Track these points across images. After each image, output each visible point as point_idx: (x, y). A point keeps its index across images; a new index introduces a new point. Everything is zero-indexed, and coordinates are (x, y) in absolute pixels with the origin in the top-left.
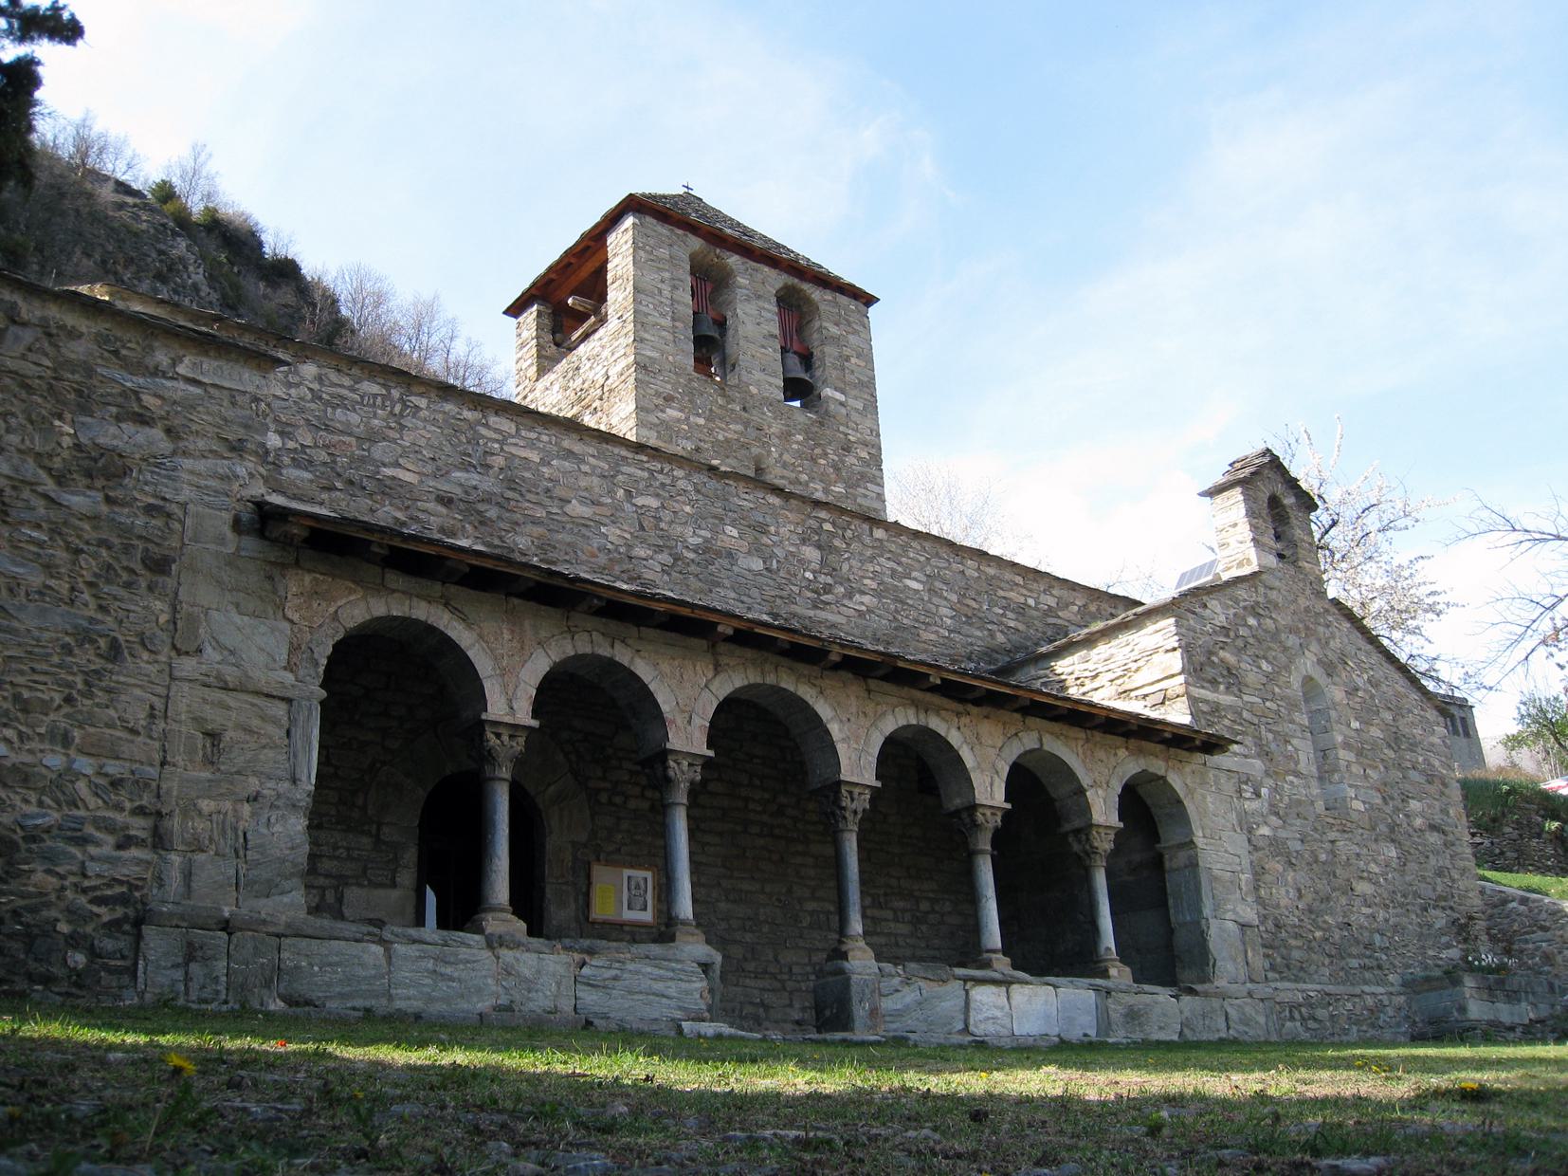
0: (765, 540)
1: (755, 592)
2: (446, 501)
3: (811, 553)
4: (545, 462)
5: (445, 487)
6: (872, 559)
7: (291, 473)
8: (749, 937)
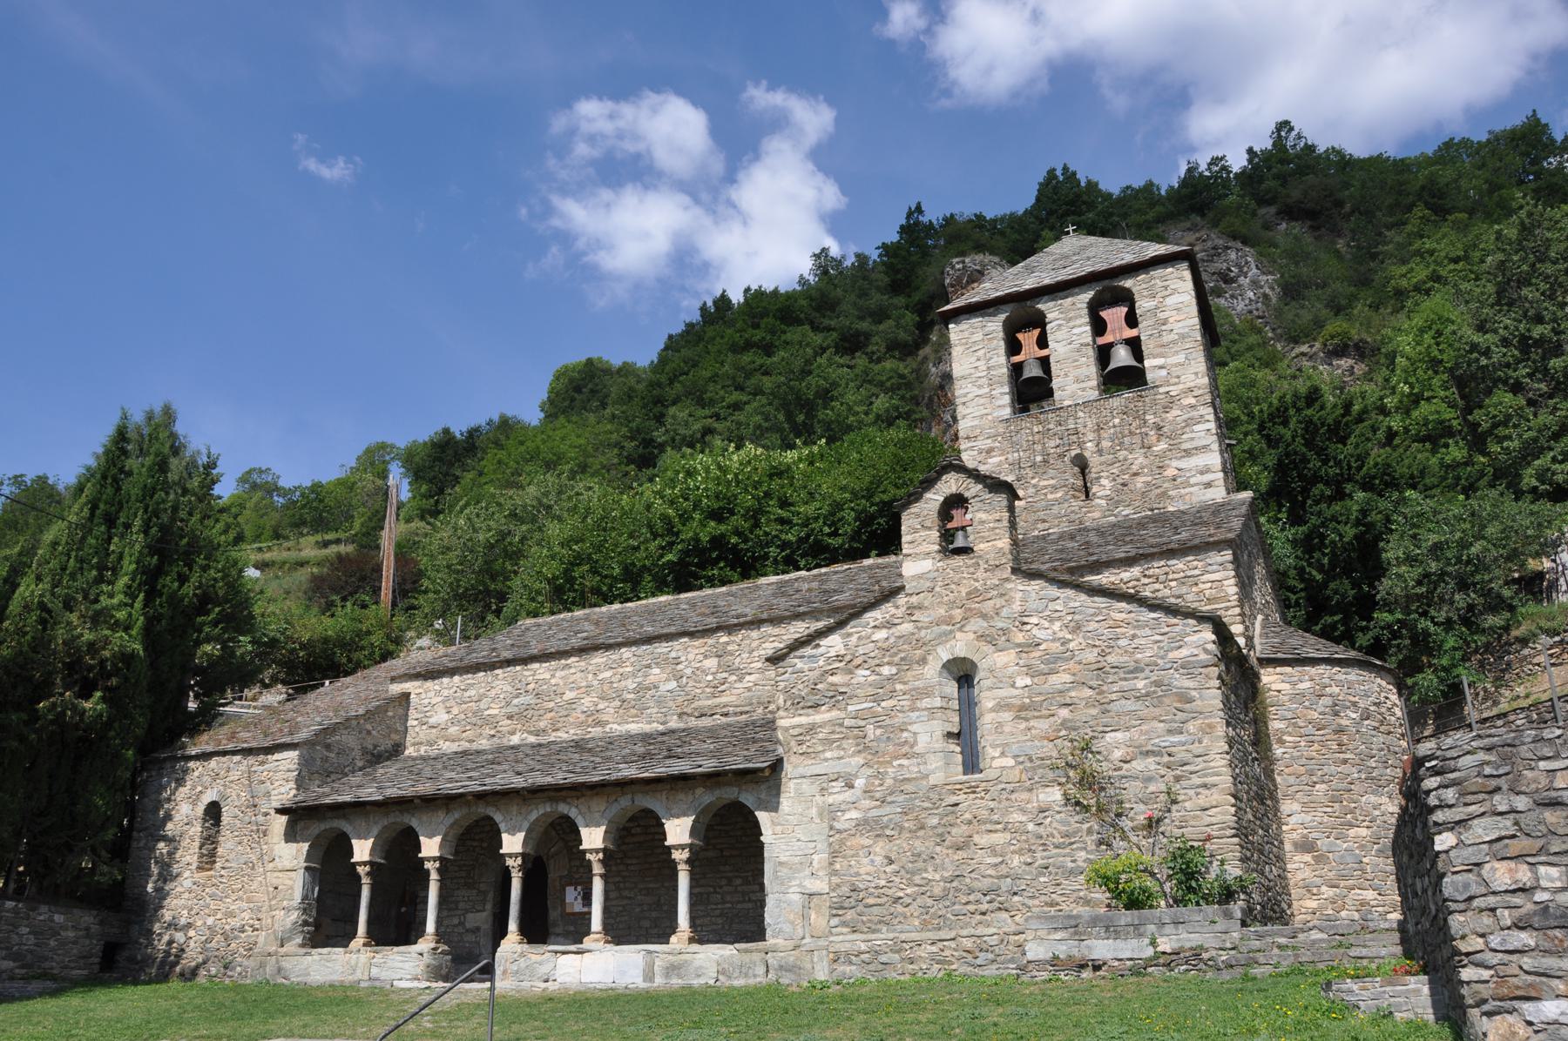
0: (680, 667)
1: (671, 704)
2: (510, 717)
3: (711, 663)
4: (553, 676)
5: (509, 710)
6: (758, 648)
7: (453, 730)
8: (654, 914)
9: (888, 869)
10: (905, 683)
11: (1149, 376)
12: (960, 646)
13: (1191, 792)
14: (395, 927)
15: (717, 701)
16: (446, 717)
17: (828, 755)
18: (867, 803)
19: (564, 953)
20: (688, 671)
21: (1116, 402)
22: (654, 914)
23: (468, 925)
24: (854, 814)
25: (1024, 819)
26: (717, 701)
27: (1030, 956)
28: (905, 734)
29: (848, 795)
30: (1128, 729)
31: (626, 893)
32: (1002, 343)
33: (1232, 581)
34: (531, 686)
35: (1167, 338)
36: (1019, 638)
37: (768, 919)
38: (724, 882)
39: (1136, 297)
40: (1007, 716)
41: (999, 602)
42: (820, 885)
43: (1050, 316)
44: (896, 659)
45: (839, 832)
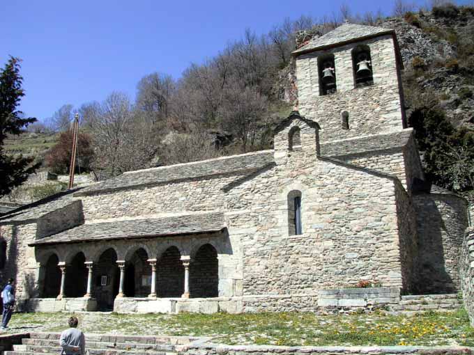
2: (120, 210)
3: (199, 190)
9: (266, 270)
10: (274, 199)
11: (375, 81)
12: (296, 185)
13: (383, 244)
14: (74, 290)
15: (201, 205)
16: (95, 209)
17: (243, 226)
18: (259, 245)
19: (141, 301)
20: (190, 193)
21: (361, 91)
22: (176, 287)
23: (104, 290)
24: (253, 249)
25: (319, 252)
26: (201, 205)
27: (319, 305)
28: (273, 219)
29: (252, 242)
30: (359, 219)
31: (165, 278)
32: (317, 67)
33: (403, 163)
34: (128, 198)
35: (382, 66)
36: (318, 183)
37: (219, 288)
38: (203, 274)
39: (371, 49)
40: (313, 213)
41: (311, 169)
42: (239, 276)
43: (336, 56)
44: (271, 190)
45: (248, 256)
